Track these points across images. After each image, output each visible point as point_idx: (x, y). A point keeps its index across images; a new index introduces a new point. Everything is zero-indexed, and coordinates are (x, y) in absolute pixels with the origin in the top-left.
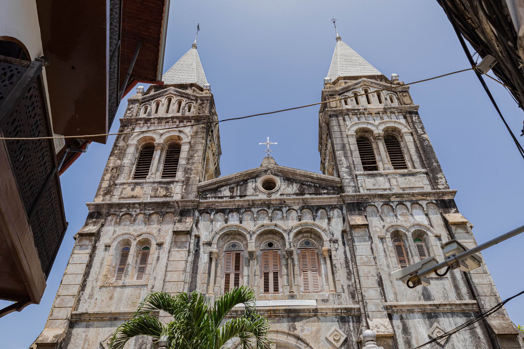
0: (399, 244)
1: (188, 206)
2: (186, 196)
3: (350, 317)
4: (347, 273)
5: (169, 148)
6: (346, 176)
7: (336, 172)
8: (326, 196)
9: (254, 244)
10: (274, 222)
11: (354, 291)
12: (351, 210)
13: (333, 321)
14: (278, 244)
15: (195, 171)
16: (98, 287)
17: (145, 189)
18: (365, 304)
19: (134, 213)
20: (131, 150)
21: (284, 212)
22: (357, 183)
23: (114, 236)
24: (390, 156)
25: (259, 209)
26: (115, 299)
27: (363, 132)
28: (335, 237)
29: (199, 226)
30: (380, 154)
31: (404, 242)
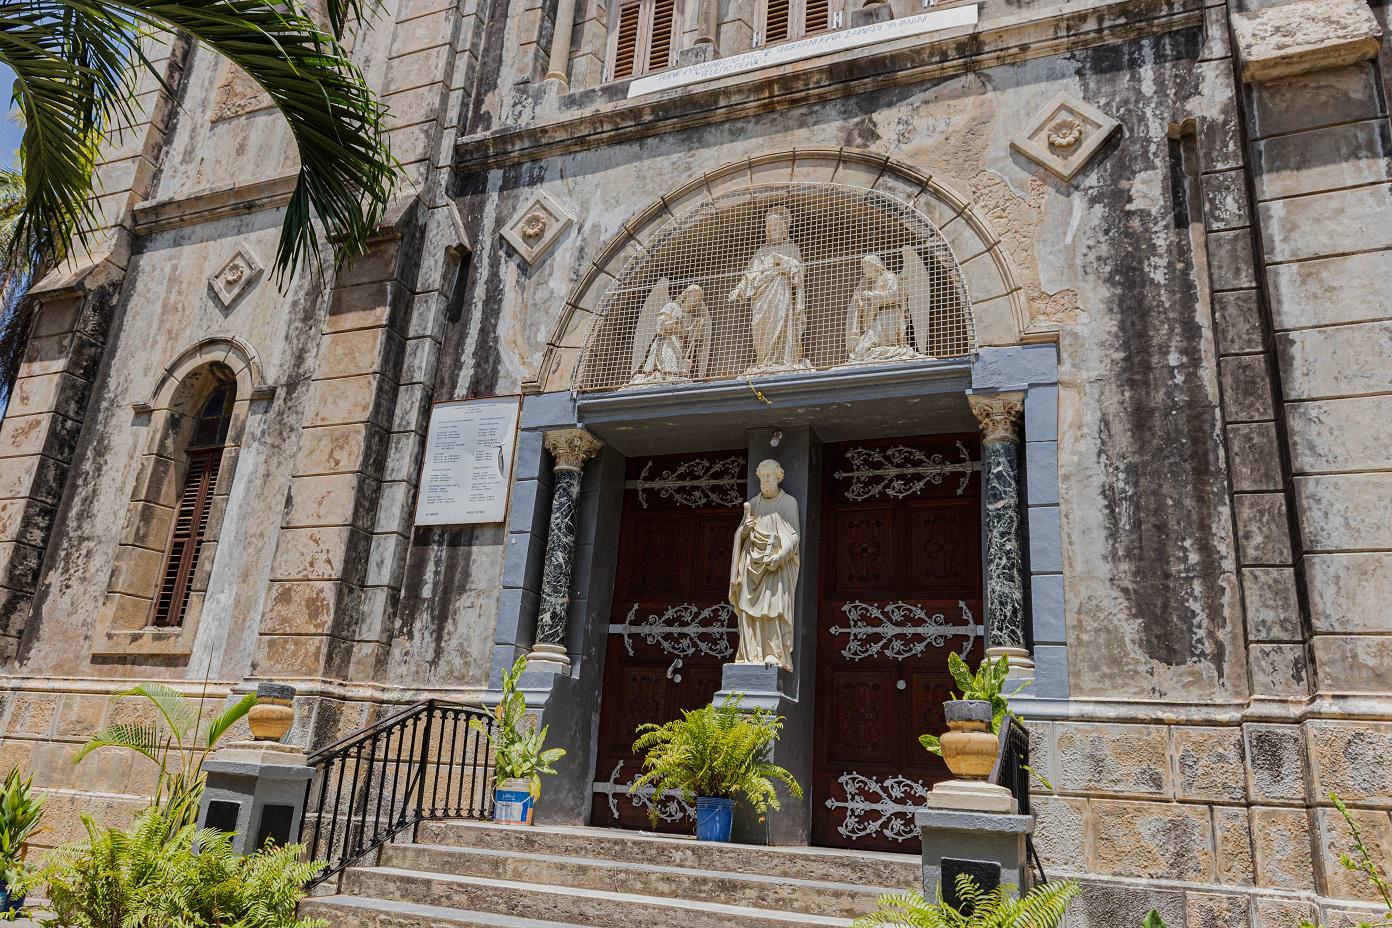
3: (1145, 42)
13: (1052, 76)
16: (208, 125)
26: (251, 152)
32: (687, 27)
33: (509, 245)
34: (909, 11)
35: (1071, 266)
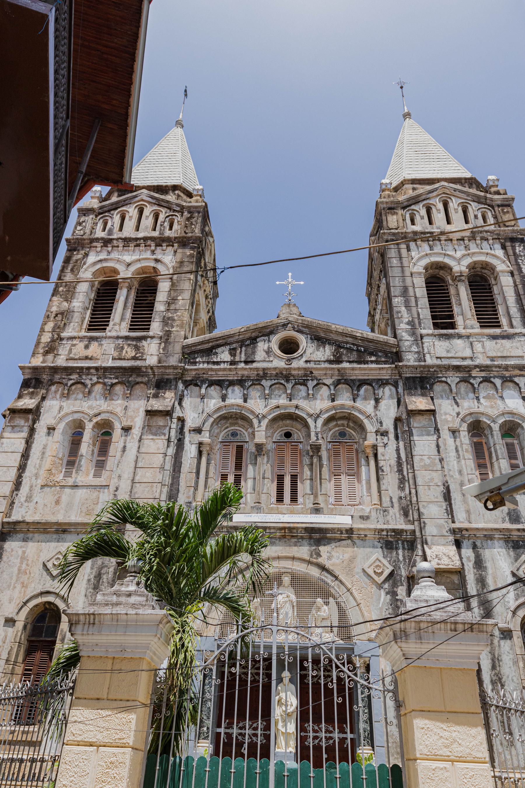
0: (479, 441)
1: (168, 375)
2: (164, 358)
4: (399, 479)
5: (140, 285)
6: (406, 336)
7: (391, 329)
8: (374, 366)
9: (264, 433)
10: (294, 402)
11: (408, 506)
12: (410, 389)
13: (374, 547)
14: (300, 434)
15: (178, 323)
17: (104, 347)
18: (422, 525)
19: (88, 382)
20: (83, 288)
21: (311, 388)
22: (423, 347)
23: (60, 415)
24: (475, 307)
25: (273, 382)
26: (63, 504)
27: (436, 268)
28: (384, 427)
29: (184, 404)
30: (460, 304)
31: (488, 438)
32: (249, 491)
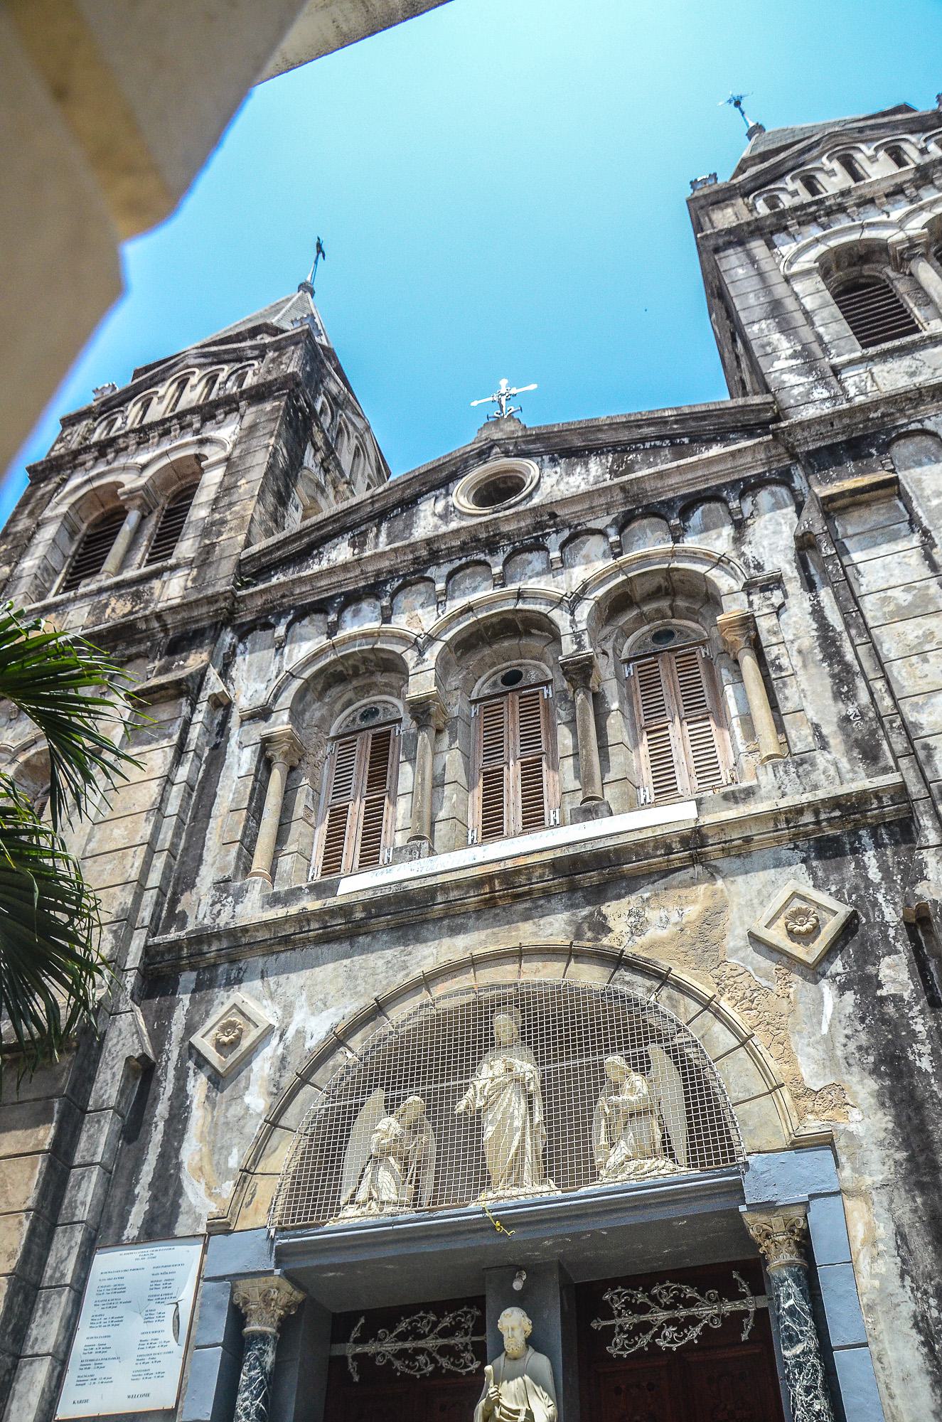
1: (197, 621)
4: (833, 676)
10: (513, 587)
11: (873, 733)
13: (778, 864)
14: (543, 666)
15: (233, 524)
17: (70, 617)
18: (922, 754)
25: (457, 563)
28: (769, 568)
29: (234, 673)
32: (399, 825)
33: (199, 1054)
34: (626, 808)
35: (832, 1058)
